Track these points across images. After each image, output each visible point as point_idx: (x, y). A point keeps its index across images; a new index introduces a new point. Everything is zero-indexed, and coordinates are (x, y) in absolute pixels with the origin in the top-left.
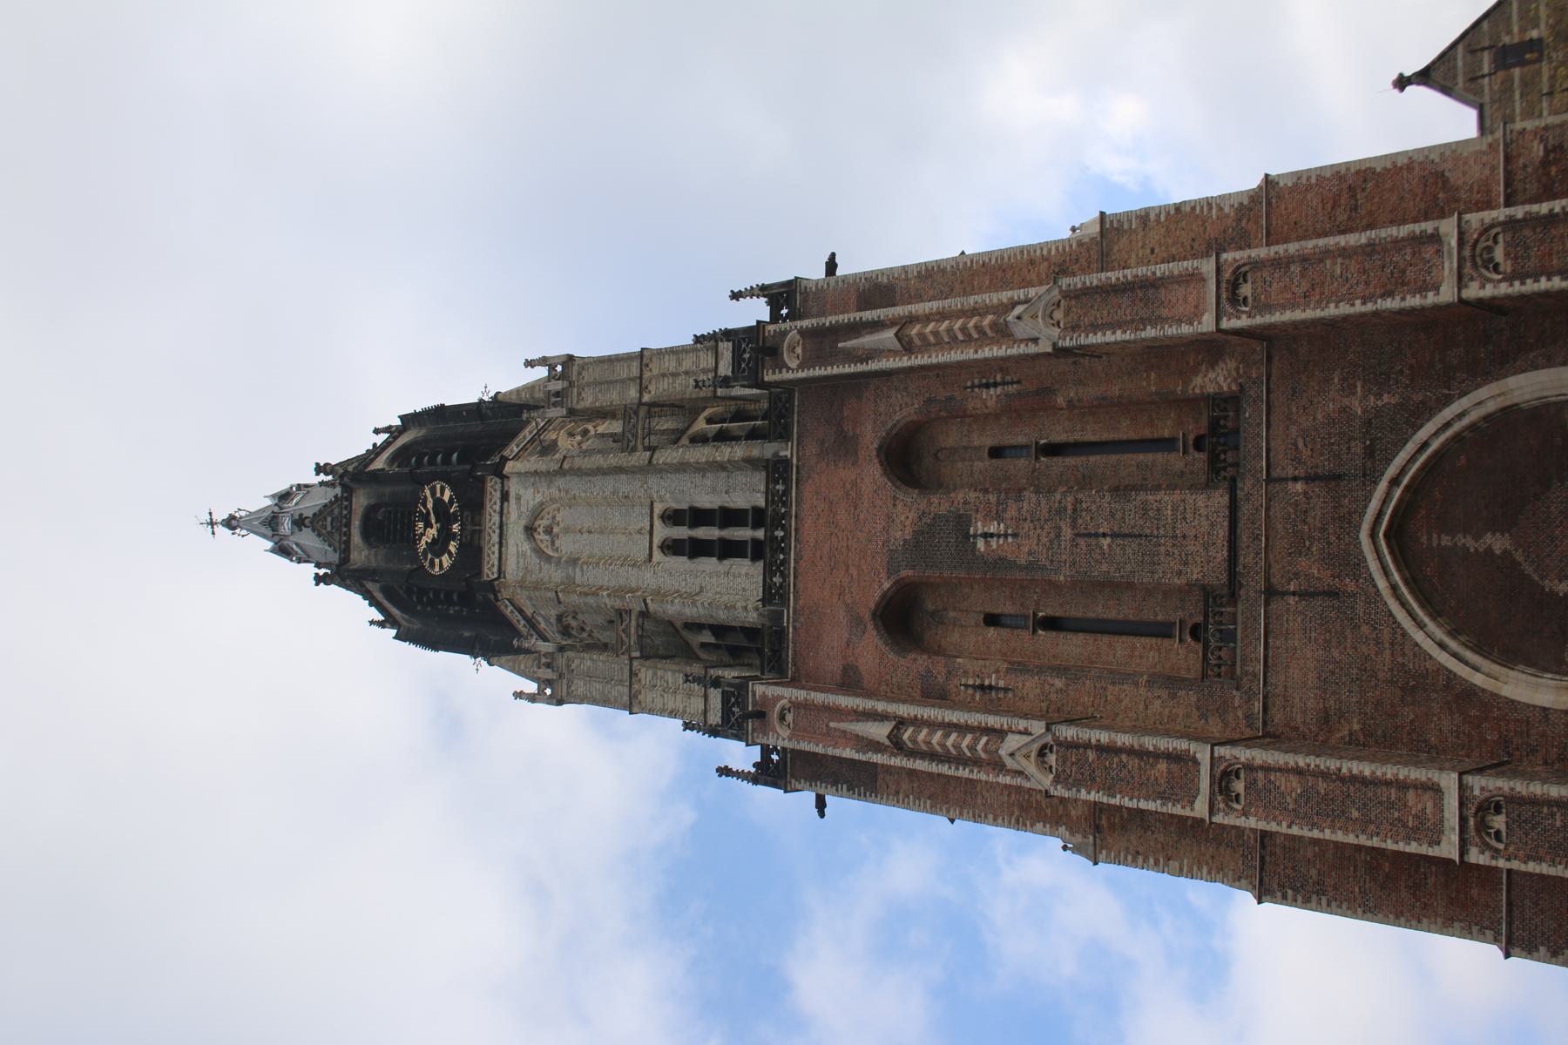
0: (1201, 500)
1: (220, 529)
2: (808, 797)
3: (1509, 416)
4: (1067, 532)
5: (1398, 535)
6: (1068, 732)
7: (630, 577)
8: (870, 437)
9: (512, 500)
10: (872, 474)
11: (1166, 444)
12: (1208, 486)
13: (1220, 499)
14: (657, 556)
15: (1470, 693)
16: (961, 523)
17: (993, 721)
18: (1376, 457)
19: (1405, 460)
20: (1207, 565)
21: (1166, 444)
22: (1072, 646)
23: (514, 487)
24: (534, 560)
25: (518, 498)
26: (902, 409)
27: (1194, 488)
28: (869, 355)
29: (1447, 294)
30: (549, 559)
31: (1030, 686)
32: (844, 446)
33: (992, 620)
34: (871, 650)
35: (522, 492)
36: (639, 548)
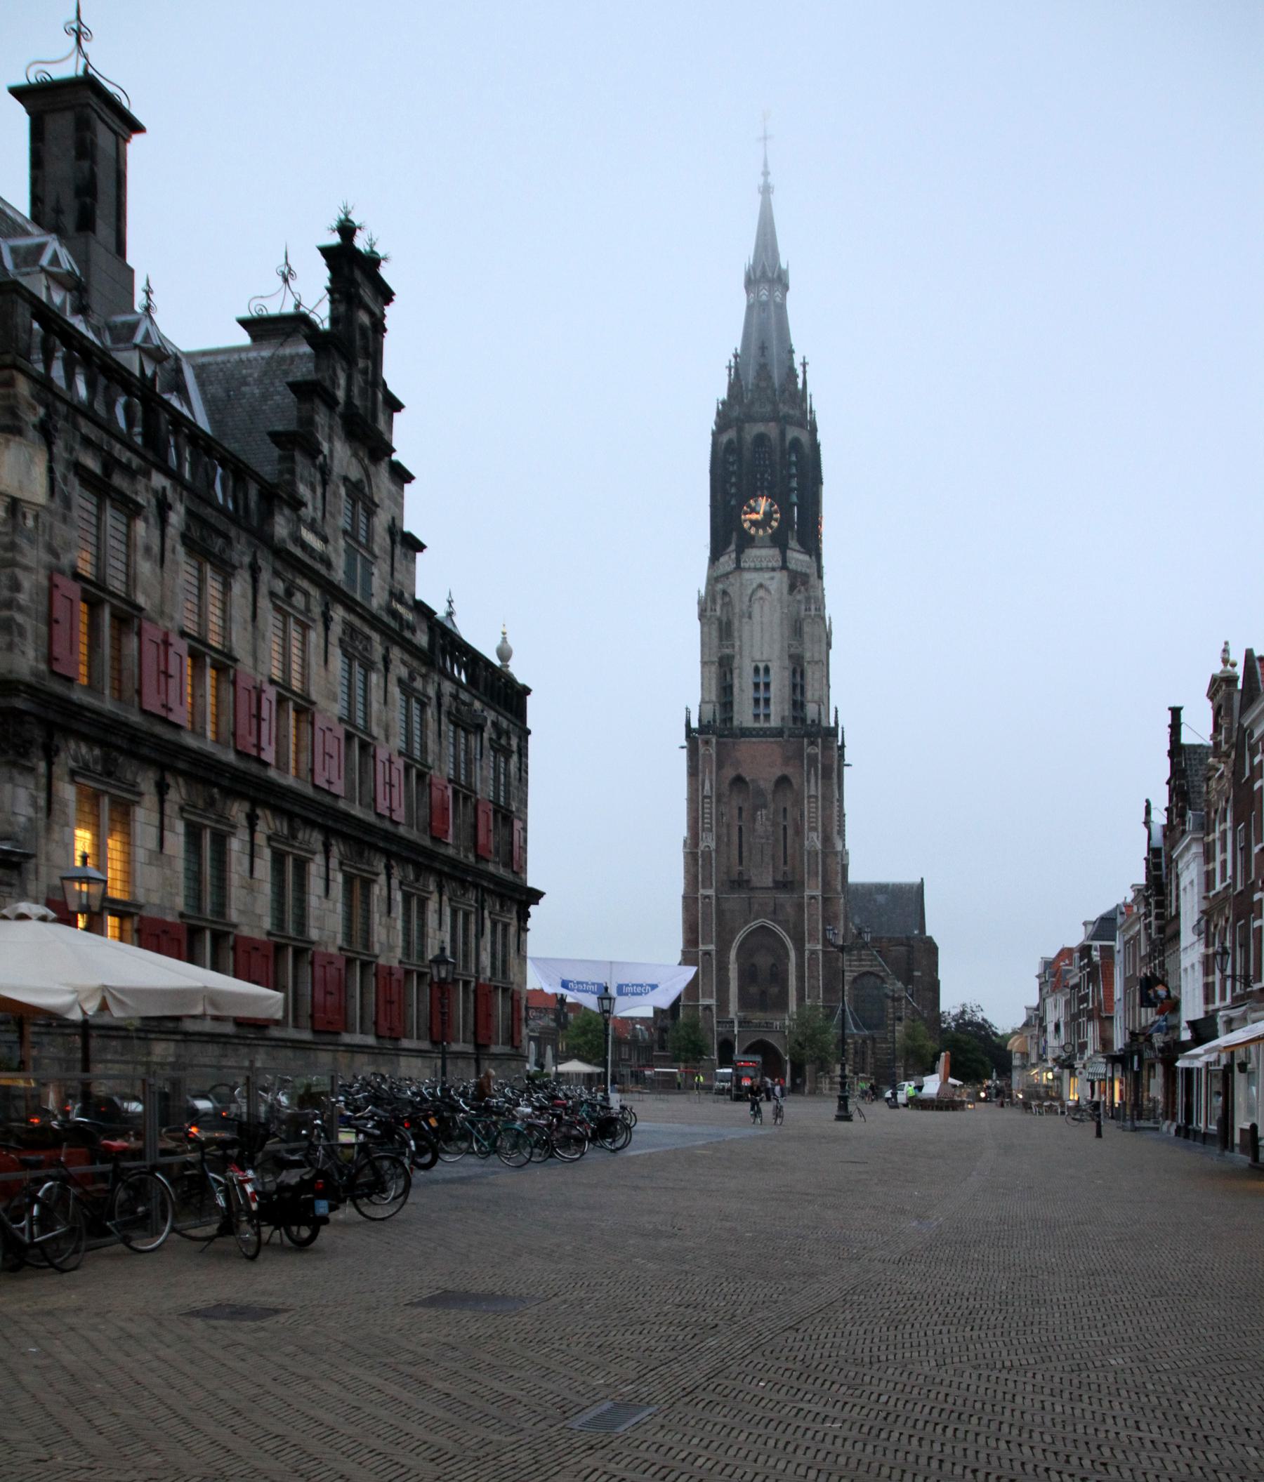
0: (770, 879)
1: (761, 181)
2: (685, 744)
3: (787, 955)
4: (764, 841)
5: (763, 928)
6: (714, 855)
7: (746, 652)
8: (789, 771)
9: (772, 574)
10: (778, 772)
11: (785, 863)
12: (775, 882)
13: (771, 885)
14: (753, 664)
15: (731, 942)
16: (765, 806)
17: (714, 829)
18: (779, 923)
19: (779, 930)
20: (756, 882)
21: (785, 863)
22: (735, 838)
23: (777, 575)
24: (749, 592)
25: (772, 578)
26: (795, 781)
27: (774, 877)
28: (809, 781)
29: (807, 946)
30: (750, 601)
31: (724, 831)
32: (786, 761)
33: (740, 809)
34: (730, 773)
35: (775, 581)
36: (757, 656)
